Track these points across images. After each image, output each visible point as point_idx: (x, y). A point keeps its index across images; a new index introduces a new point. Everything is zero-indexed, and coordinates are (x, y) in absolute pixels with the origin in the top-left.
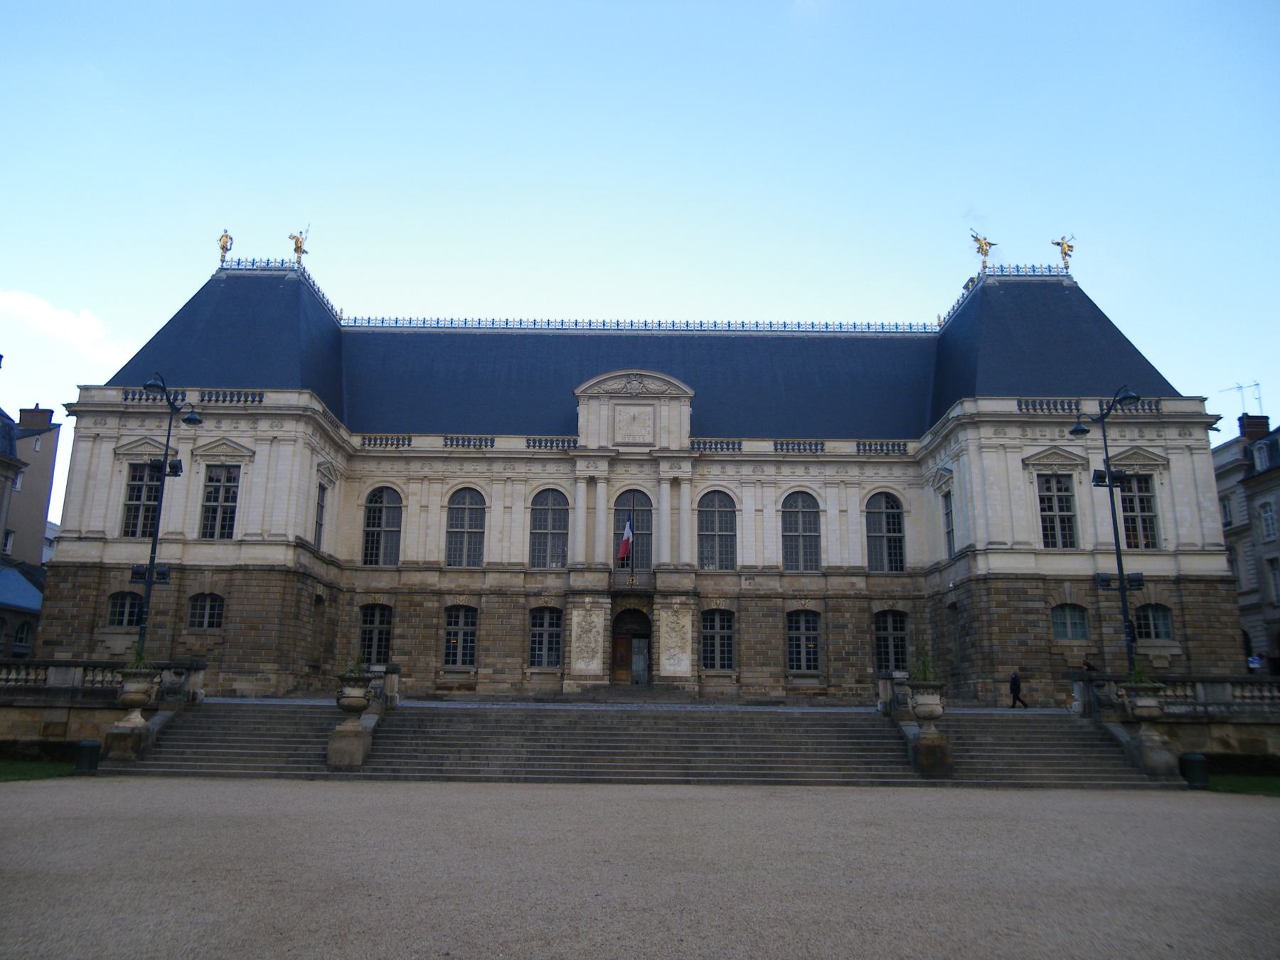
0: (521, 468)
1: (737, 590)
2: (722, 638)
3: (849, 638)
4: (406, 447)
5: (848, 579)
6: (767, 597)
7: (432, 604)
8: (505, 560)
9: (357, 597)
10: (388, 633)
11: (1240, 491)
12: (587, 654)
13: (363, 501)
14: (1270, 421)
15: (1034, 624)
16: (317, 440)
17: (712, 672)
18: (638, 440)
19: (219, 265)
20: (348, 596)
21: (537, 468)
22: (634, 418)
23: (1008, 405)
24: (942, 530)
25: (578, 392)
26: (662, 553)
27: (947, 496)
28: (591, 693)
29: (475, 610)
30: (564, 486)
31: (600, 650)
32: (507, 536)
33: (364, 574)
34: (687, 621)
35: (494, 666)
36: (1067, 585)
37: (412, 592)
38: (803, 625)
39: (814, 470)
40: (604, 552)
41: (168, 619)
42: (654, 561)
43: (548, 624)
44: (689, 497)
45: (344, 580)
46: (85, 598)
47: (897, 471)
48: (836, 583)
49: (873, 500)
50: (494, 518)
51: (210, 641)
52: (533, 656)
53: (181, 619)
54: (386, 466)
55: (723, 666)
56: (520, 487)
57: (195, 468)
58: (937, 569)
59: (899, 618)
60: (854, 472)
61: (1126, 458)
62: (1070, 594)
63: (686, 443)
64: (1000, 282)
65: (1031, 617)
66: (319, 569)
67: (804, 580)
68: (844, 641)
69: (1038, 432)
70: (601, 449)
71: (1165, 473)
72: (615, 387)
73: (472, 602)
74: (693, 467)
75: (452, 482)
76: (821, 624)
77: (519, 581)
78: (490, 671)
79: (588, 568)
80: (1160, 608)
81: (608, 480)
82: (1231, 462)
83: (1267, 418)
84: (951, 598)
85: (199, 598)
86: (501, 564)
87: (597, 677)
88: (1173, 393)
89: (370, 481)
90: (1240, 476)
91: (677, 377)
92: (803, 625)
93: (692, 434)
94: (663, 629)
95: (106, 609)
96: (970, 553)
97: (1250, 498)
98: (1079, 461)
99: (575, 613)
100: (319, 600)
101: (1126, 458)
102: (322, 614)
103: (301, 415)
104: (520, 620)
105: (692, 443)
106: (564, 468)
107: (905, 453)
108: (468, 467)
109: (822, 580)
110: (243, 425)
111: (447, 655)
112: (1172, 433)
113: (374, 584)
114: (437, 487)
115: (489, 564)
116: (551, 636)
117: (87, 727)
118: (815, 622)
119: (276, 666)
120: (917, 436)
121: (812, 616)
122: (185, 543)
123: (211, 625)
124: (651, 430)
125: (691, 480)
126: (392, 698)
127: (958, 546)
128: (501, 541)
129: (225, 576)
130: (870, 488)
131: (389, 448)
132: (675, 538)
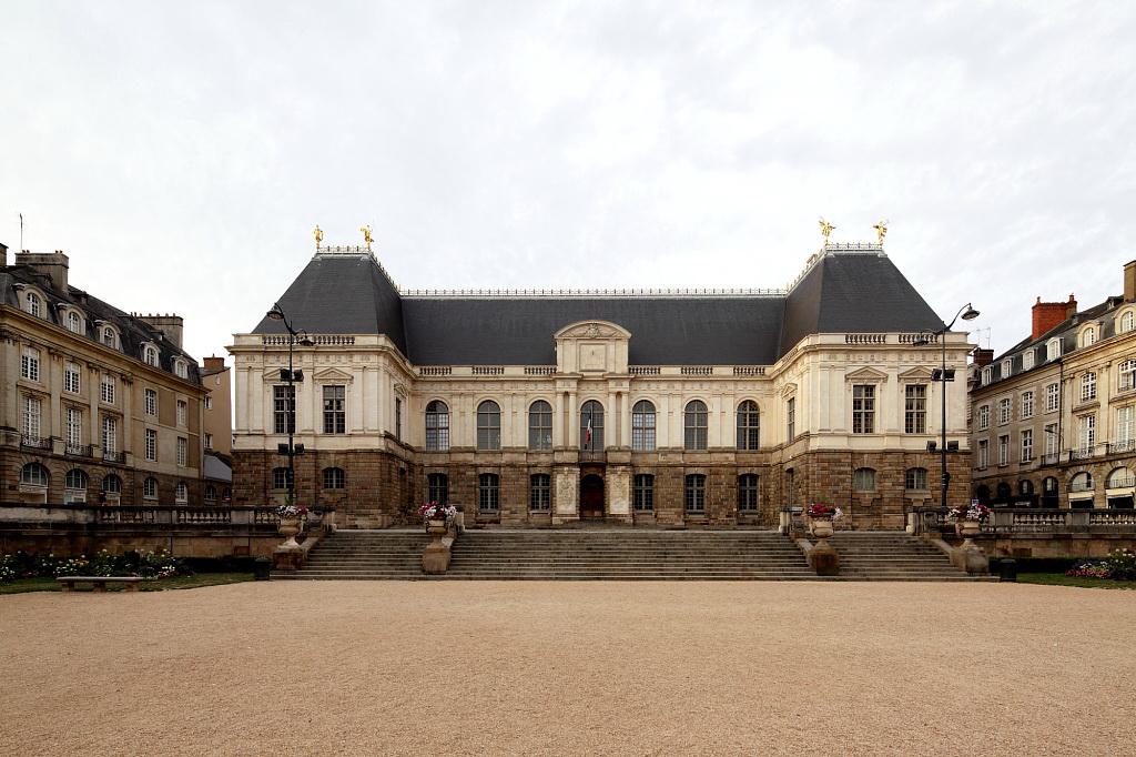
0: (522, 387)
2: (646, 491)
3: (723, 490)
6: (675, 466)
7: (471, 473)
9: (425, 469)
12: (566, 500)
15: (844, 481)
17: (641, 511)
18: (595, 368)
24: (786, 423)
25: (556, 336)
26: (609, 440)
28: (568, 524)
31: (574, 498)
32: (515, 431)
34: (626, 481)
36: (866, 456)
37: (458, 465)
38: (695, 483)
39: (706, 386)
40: (574, 440)
41: (311, 484)
42: (606, 445)
43: (540, 488)
44: (626, 405)
45: (417, 459)
46: (258, 472)
47: (758, 386)
48: (717, 458)
50: (506, 420)
51: (339, 496)
52: (533, 503)
53: (319, 484)
54: (437, 387)
55: (646, 508)
56: (522, 399)
58: (781, 448)
59: (754, 478)
60: (731, 386)
62: (867, 462)
63: (625, 368)
65: (842, 476)
66: (401, 452)
67: (698, 456)
70: (572, 373)
76: (706, 483)
78: (507, 512)
80: (922, 470)
81: (577, 394)
85: (328, 471)
86: (512, 448)
87: (572, 515)
92: (695, 483)
93: (629, 364)
94: (612, 486)
95: (272, 478)
99: (559, 476)
100: (402, 471)
102: (405, 480)
104: (524, 482)
108: (488, 386)
111: (482, 503)
115: (504, 448)
116: (543, 491)
117: (261, 549)
118: (703, 481)
119: (380, 511)
121: (701, 478)
122: (316, 436)
123: (338, 486)
126: (461, 527)
127: (797, 433)
129: (343, 456)
132: (617, 430)
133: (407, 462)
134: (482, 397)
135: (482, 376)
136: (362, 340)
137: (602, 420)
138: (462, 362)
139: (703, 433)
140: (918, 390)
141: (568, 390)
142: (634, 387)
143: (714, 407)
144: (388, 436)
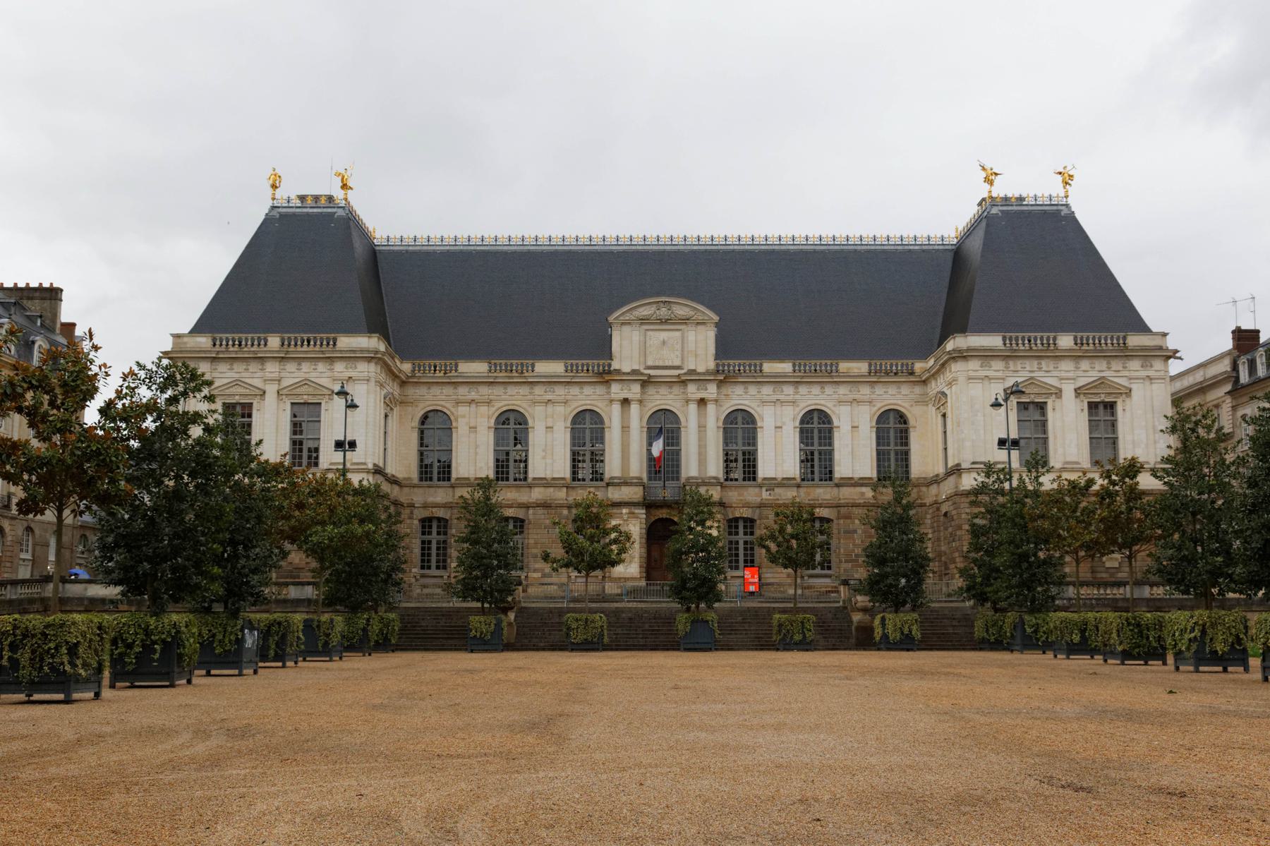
0: (560, 391)
1: (759, 500)
4: (453, 373)
5: (859, 489)
8: (549, 476)
9: (416, 511)
10: (445, 542)
11: (1228, 400)
13: (416, 423)
14: (1261, 335)
16: (383, 377)
19: (270, 203)
20: (408, 511)
21: (575, 390)
22: (664, 343)
23: (994, 341)
24: (941, 446)
25: (611, 319)
27: (944, 415)
29: (522, 521)
30: (600, 407)
32: (549, 454)
33: (421, 490)
35: (541, 570)
39: (829, 390)
40: (637, 468)
44: (714, 418)
47: (905, 390)
48: (847, 493)
49: (883, 417)
50: (537, 438)
54: (436, 390)
56: (560, 409)
57: (282, 405)
58: (936, 480)
60: (865, 391)
61: (1095, 387)
63: (711, 365)
64: (1002, 211)
66: (386, 487)
67: (819, 491)
68: (854, 545)
69: (1019, 364)
70: (634, 372)
71: (1128, 400)
72: (645, 313)
73: (520, 514)
74: (718, 387)
75: (498, 405)
77: (561, 495)
78: (539, 575)
79: (625, 483)
81: (641, 402)
82: (1221, 374)
83: (1258, 331)
84: (944, 508)
88: (1143, 328)
89: (421, 405)
90: (1228, 387)
91: (702, 303)
96: (957, 471)
97: (1234, 408)
98: (1053, 390)
101: (1095, 387)
103: (372, 357)
105: (717, 365)
106: (600, 390)
107: (912, 373)
108: (512, 390)
109: (836, 490)
110: (321, 367)
112: (1135, 365)
113: (431, 500)
114: (484, 409)
115: (534, 479)
120: (924, 357)
124: (678, 353)
125: (716, 401)
127: (950, 464)
128: (544, 458)
130: (880, 406)
131: (438, 374)
132: (702, 456)
133: (396, 503)
134: (501, 405)
135: (502, 376)
136: (345, 342)
137: (678, 438)
138: (472, 356)
139: (828, 457)
140: (1105, 407)
141: (629, 396)
142: (724, 390)
143: (842, 419)
144: (378, 471)
